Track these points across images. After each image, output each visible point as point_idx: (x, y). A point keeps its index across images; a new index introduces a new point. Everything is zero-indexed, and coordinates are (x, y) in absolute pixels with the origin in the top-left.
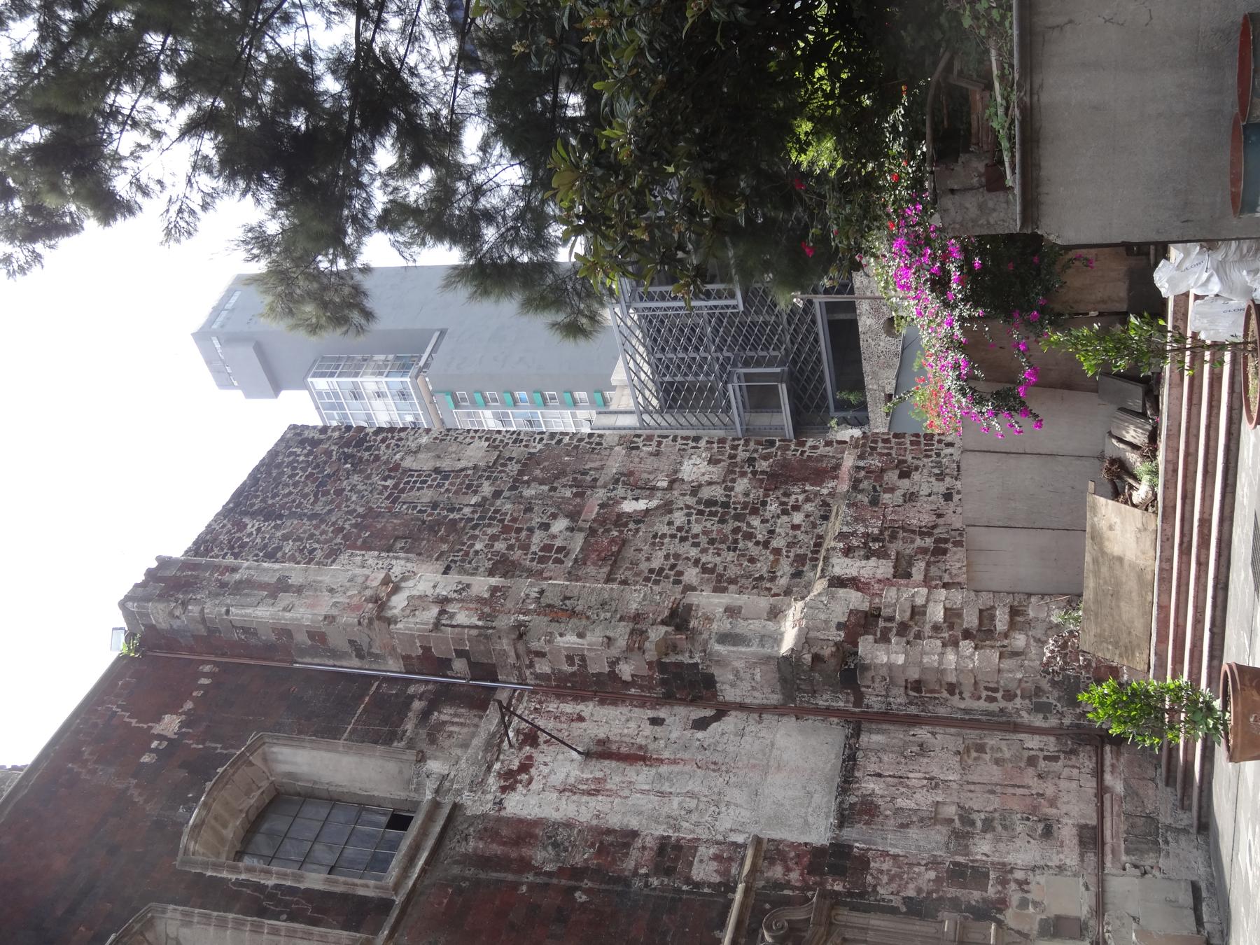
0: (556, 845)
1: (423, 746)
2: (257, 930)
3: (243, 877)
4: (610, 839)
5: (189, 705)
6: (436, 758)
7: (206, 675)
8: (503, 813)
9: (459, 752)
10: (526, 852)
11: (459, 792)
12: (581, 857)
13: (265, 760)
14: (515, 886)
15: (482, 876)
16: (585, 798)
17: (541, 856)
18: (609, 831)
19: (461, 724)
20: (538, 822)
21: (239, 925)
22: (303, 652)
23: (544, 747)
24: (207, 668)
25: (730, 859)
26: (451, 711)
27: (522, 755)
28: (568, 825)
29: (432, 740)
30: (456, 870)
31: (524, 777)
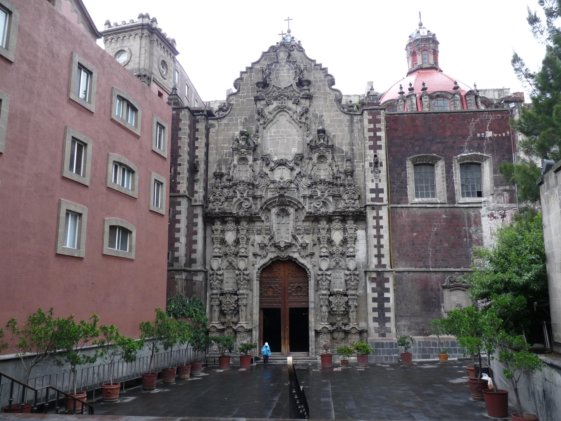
0: (476, 231)
1: (496, 194)
2: (443, 181)
3: (454, 172)
4: (480, 241)
5: (495, 135)
6: (493, 198)
7: (506, 134)
8: (482, 217)
9: (496, 201)
10: (473, 225)
11: (485, 206)
12: (474, 237)
13: (485, 160)
14: (465, 226)
15: (465, 219)
16: (489, 233)
17: (473, 228)
18: (482, 240)
19: (504, 200)
20: (481, 225)
21: (443, 177)
22: (516, 154)
23: (501, 220)
24: (508, 133)
25: (480, 266)
26: (507, 195)
27: (498, 216)
28: (482, 232)
29: (497, 195)
30: (466, 213)
31: (492, 218)
